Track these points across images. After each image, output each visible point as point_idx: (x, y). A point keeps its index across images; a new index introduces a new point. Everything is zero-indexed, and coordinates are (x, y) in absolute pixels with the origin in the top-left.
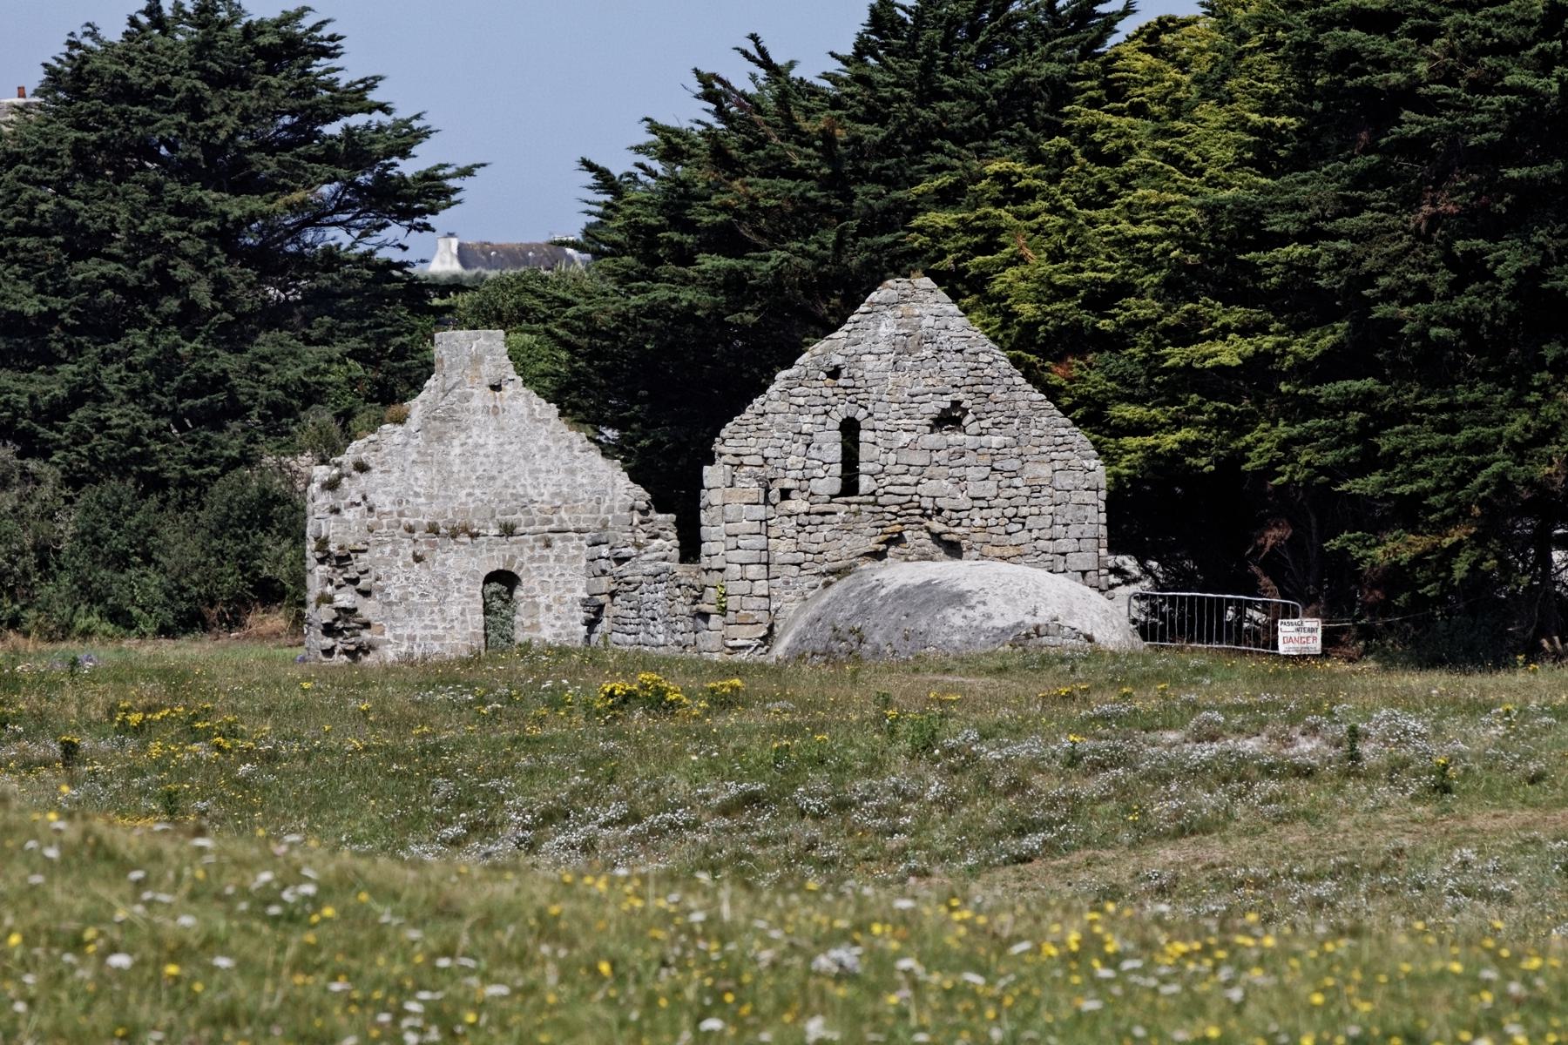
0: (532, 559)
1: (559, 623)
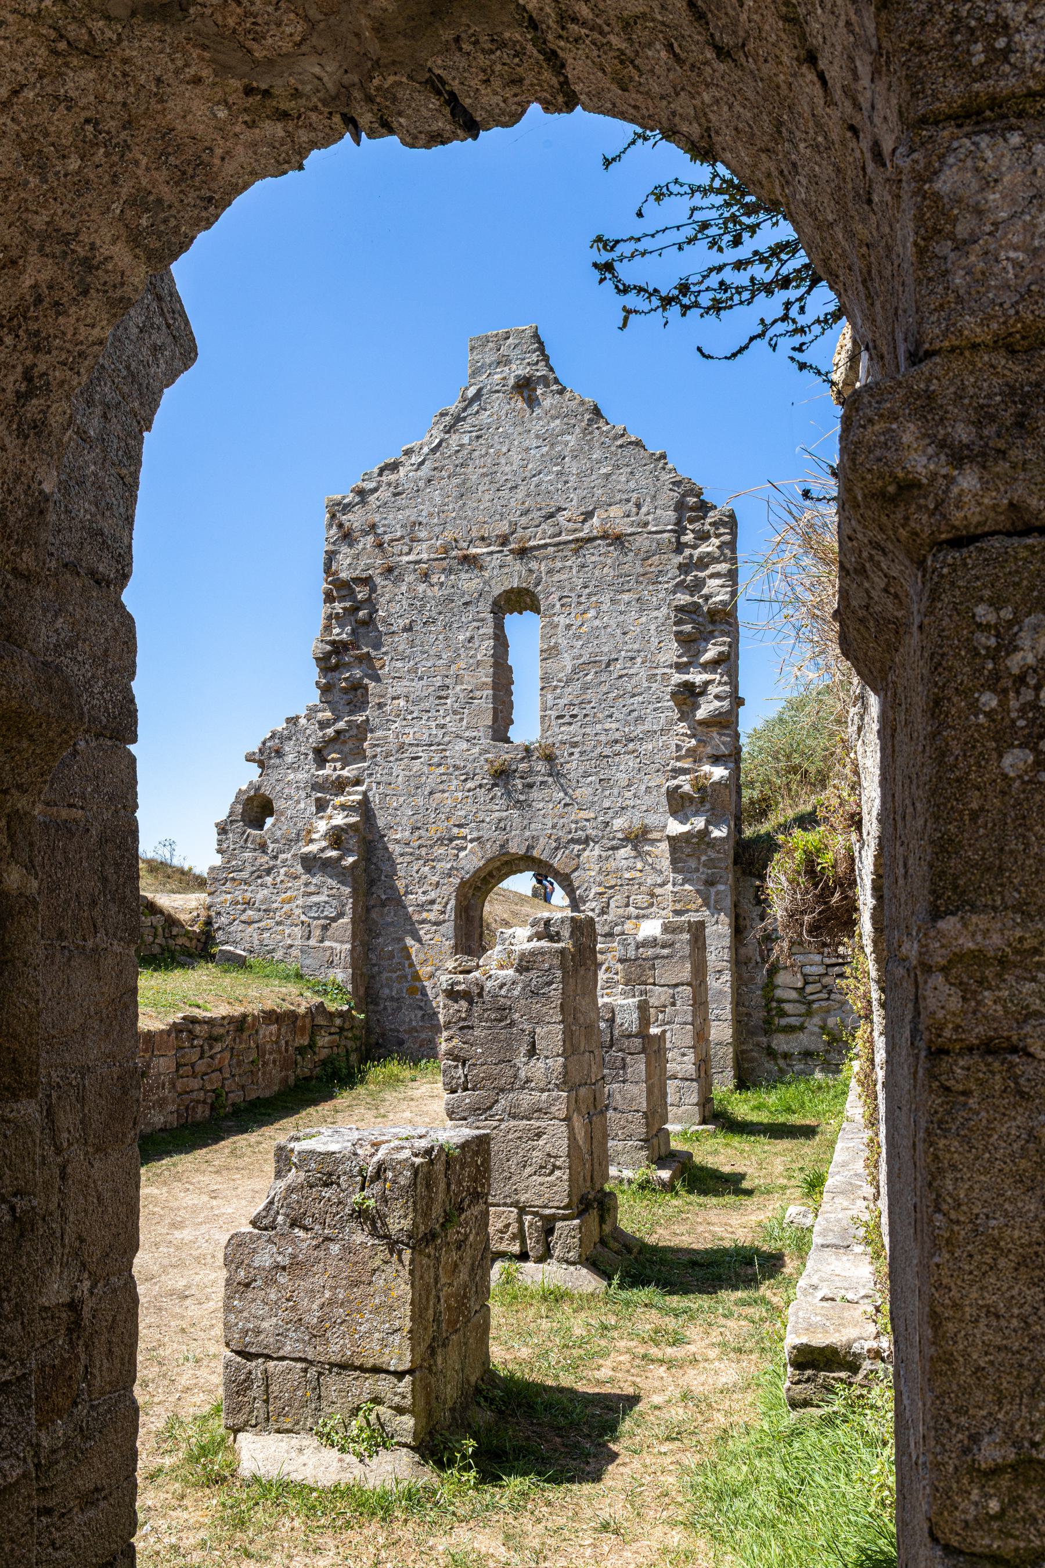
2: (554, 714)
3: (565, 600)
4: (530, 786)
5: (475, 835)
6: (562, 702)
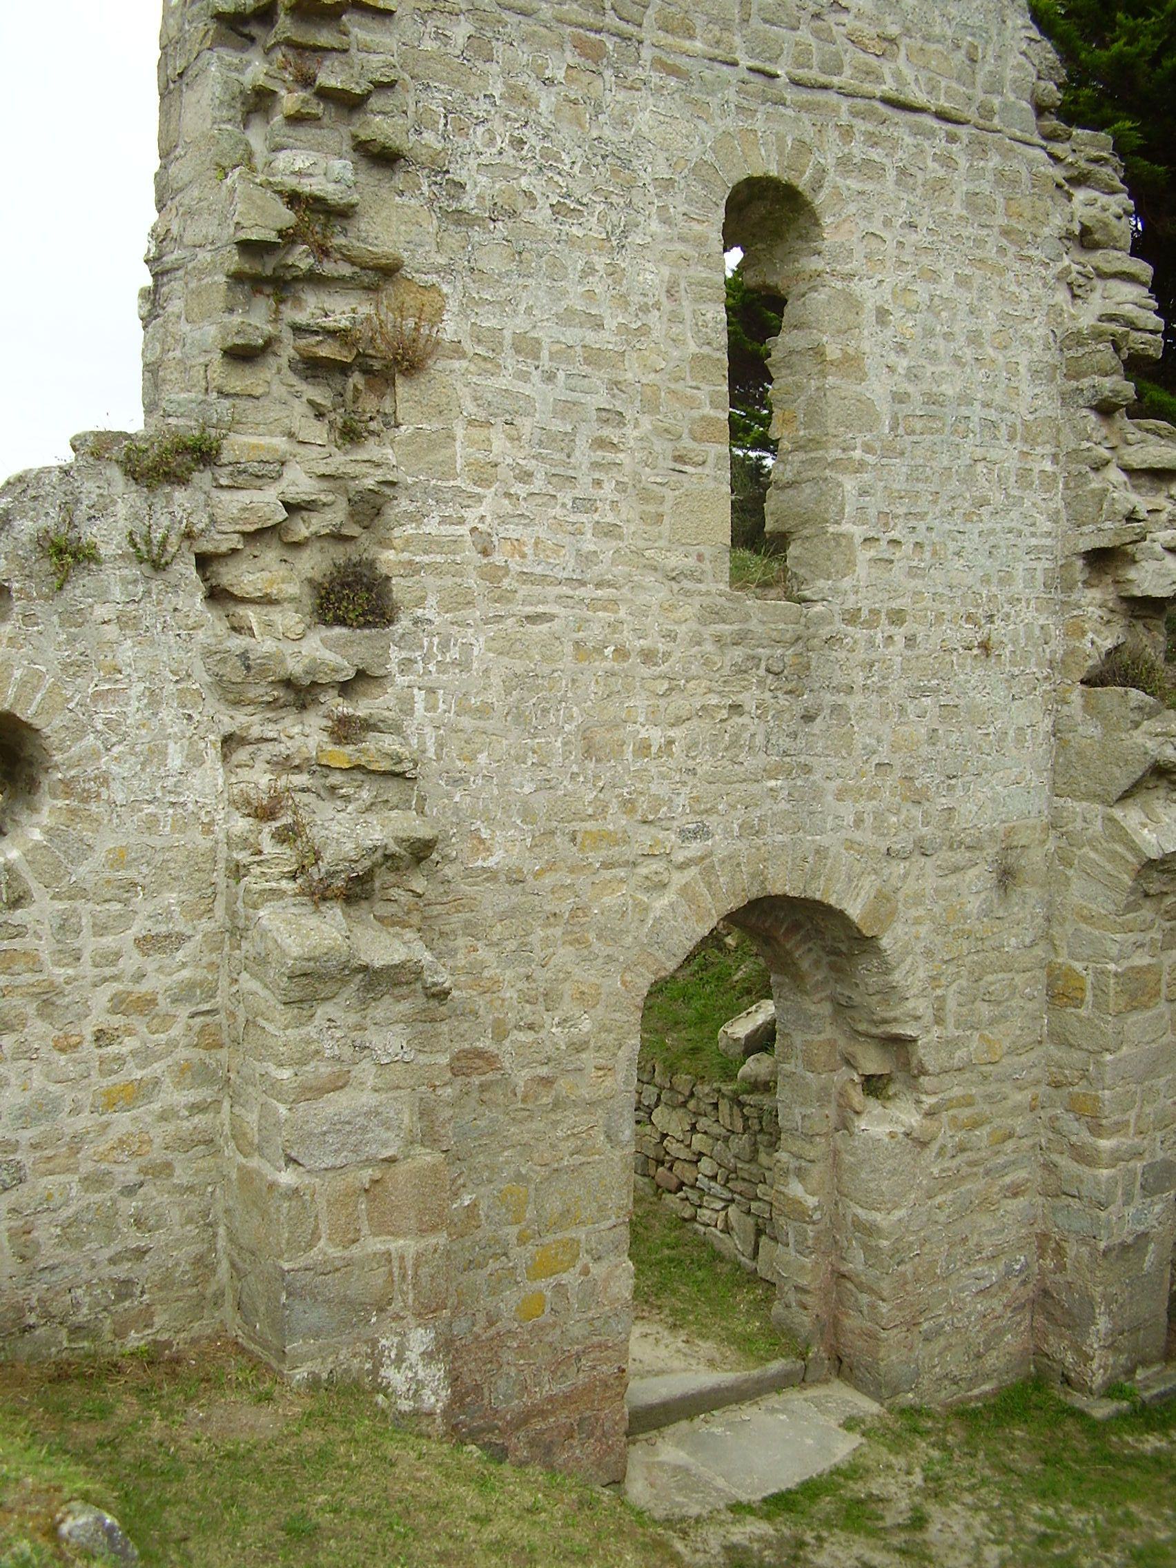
0: (844, 163)
1: (903, 363)
2: (858, 532)
3: (874, 244)
4: (808, 718)
5: (695, 848)
6: (874, 504)
